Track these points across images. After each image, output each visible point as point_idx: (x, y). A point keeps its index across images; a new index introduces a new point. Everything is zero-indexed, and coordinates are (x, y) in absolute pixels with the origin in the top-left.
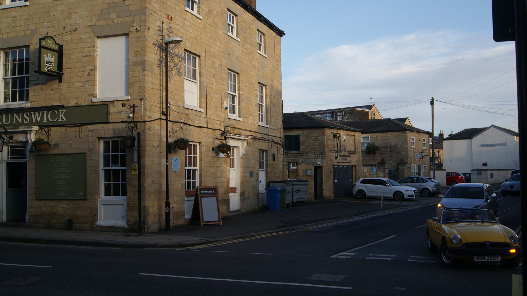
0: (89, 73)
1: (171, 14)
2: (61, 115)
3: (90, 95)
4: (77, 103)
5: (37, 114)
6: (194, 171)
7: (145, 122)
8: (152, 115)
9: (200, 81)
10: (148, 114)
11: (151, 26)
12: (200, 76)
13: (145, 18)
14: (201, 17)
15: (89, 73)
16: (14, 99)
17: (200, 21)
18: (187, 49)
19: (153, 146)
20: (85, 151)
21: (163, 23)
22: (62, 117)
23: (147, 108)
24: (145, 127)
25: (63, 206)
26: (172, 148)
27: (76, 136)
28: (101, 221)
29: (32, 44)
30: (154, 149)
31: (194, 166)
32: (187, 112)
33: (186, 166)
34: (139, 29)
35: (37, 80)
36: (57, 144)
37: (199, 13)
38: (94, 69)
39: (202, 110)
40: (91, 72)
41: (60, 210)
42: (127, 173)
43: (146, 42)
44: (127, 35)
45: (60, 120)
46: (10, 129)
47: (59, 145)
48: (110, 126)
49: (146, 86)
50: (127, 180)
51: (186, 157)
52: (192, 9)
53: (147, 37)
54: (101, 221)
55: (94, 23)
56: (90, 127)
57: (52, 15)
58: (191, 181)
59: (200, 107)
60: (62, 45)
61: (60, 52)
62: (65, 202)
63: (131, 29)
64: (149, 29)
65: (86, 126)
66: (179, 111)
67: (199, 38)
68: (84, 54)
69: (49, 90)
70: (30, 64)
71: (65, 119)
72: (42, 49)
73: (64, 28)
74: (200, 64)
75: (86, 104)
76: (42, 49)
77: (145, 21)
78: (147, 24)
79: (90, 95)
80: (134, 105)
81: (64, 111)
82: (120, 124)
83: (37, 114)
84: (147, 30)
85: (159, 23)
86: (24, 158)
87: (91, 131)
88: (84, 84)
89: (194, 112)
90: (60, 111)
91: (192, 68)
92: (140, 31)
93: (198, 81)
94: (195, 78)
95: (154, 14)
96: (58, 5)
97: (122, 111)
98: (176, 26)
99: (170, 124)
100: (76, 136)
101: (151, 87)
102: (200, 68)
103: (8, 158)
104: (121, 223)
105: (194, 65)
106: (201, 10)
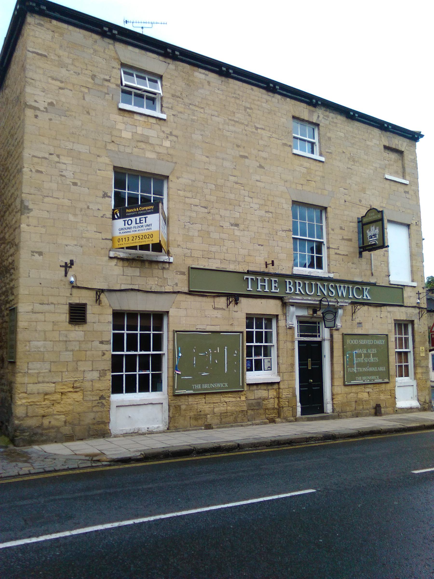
0: (384, 253)
2: (365, 293)
5: (342, 288)
15: (384, 253)
16: (311, 266)
22: (367, 295)
25: (368, 390)
27: (377, 316)
28: (401, 404)
31: (406, 348)
35: (338, 249)
36: (360, 323)
40: (386, 252)
41: (364, 396)
44: (408, 226)
47: (363, 324)
48: (403, 309)
54: (401, 404)
65: (385, 307)
69: (350, 263)
71: (369, 298)
73: (360, 201)
75: (383, 285)
82: (411, 308)
83: (342, 288)
86: (316, 336)
87: (389, 312)
88: (381, 264)
96: (352, 174)
97: (411, 297)
100: (377, 316)
104: (415, 404)
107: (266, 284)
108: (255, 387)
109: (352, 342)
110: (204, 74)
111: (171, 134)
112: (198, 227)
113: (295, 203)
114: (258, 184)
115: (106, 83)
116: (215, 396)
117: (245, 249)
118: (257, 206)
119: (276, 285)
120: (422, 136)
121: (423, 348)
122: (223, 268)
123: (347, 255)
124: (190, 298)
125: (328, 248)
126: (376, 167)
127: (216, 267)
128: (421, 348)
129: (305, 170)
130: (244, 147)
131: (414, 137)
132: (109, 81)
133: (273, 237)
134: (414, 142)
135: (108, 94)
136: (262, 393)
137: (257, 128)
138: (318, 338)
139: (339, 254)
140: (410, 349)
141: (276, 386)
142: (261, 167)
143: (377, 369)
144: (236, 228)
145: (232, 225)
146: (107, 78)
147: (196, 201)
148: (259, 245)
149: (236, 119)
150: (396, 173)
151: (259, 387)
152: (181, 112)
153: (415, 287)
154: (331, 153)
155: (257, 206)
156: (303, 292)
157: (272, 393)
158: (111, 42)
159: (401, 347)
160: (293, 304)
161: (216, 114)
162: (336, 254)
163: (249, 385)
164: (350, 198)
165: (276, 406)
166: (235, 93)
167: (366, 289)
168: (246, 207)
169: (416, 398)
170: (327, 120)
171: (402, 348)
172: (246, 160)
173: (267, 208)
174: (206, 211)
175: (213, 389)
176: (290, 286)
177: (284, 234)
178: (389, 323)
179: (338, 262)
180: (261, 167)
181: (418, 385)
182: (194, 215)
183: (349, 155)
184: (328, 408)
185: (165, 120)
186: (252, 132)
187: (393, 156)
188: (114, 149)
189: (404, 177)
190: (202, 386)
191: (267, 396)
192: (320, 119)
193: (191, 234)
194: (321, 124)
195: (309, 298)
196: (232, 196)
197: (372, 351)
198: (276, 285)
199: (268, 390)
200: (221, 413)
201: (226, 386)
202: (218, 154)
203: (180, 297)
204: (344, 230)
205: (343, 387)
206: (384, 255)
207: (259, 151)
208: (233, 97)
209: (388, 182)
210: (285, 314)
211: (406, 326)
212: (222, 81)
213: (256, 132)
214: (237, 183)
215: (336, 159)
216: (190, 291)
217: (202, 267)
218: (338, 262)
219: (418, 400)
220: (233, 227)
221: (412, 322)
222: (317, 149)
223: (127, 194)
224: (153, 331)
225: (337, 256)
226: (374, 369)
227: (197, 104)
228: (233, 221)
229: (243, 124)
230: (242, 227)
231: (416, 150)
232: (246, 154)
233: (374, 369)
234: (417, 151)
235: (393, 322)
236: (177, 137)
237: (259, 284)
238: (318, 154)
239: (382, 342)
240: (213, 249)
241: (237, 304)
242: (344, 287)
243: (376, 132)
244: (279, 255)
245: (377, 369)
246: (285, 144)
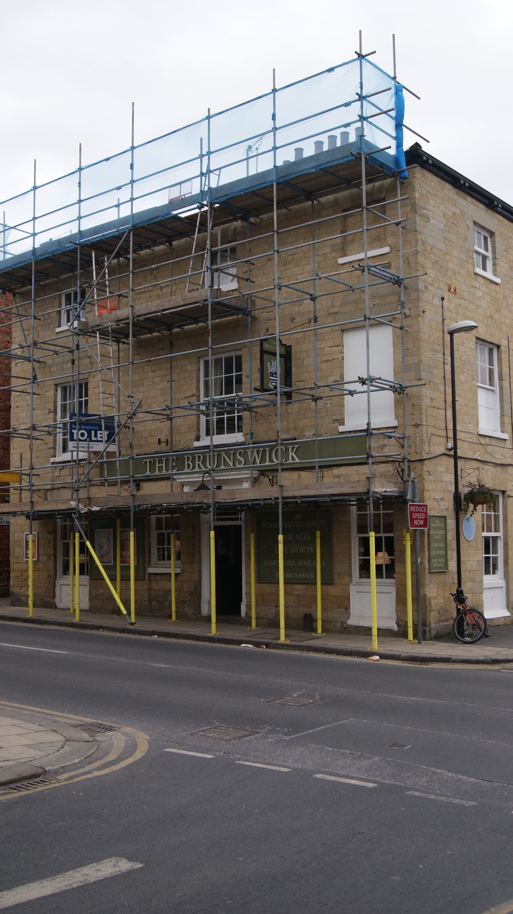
1: (455, 284)
3: (335, 421)
5: (255, 454)
6: (495, 539)
7: (422, 460)
8: (432, 449)
9: (501, 388)
10: (426, 447)
11: (427, 308)
12: (501, 379)
13: (418, 295)
14: (498, 280)
16: (220, 431)
17: (497, 288)
18: (481, 337)
19: (434, 499)
21: (443, 299)
23: (425, 438)
24: (422, 470)
26: (462, 502)
30: (436, 504)
32: (483, 441)
33: (483, 531)
37: (495, 275)
39: (506, 436)
42: (395, 543)
43: (421, 334)
45: (290, 461)
46: (219, 476)
49: (423, 404)
50: (396, 553)
51: (483, 515)
52: (484, 268)
53: (421, 326)
55: (337, 309)
56: (336, 471)
58: (491, 555)
59: (503, 432)
60: (290, 346)
61: (287, 356)
64: (424, 312)
66: (471, 440)
67: (497, 316)
68: (324, 359)
70: (244, 377)
71: (297, 460)
72: (265, 355)
73: (292, 319)
74: (500, 360)
76: (265, 356)
77: (418, 300)
78: (421, 304)
79: (335, 421)
81: (296, 446)
84: (422, 313)
85: (437, 301)
89: (493, 442)
90: (290, 447)
91: (487, 366)
92: (409, 316)
93: (497, 388)
94: (491, 383)
95: (430, 287)
97: (385, 445)
98: (462, 301)
99: (460, 463)
101: (429, 404)
102: (500, 366)
105: (491, 363)
106: (498, 269)
107: (164, 465)
108: (159, 576)
118: (160, 378)
119: (174, 464)
151: (164, 576)
155: (160, 378)
159: (489, 530)
163: (150, 574)
167: (293, 448)
176: (189, 462)
195: (196, 475)
197: (303, 537)
237: (157, 465)
242: (258, 452)
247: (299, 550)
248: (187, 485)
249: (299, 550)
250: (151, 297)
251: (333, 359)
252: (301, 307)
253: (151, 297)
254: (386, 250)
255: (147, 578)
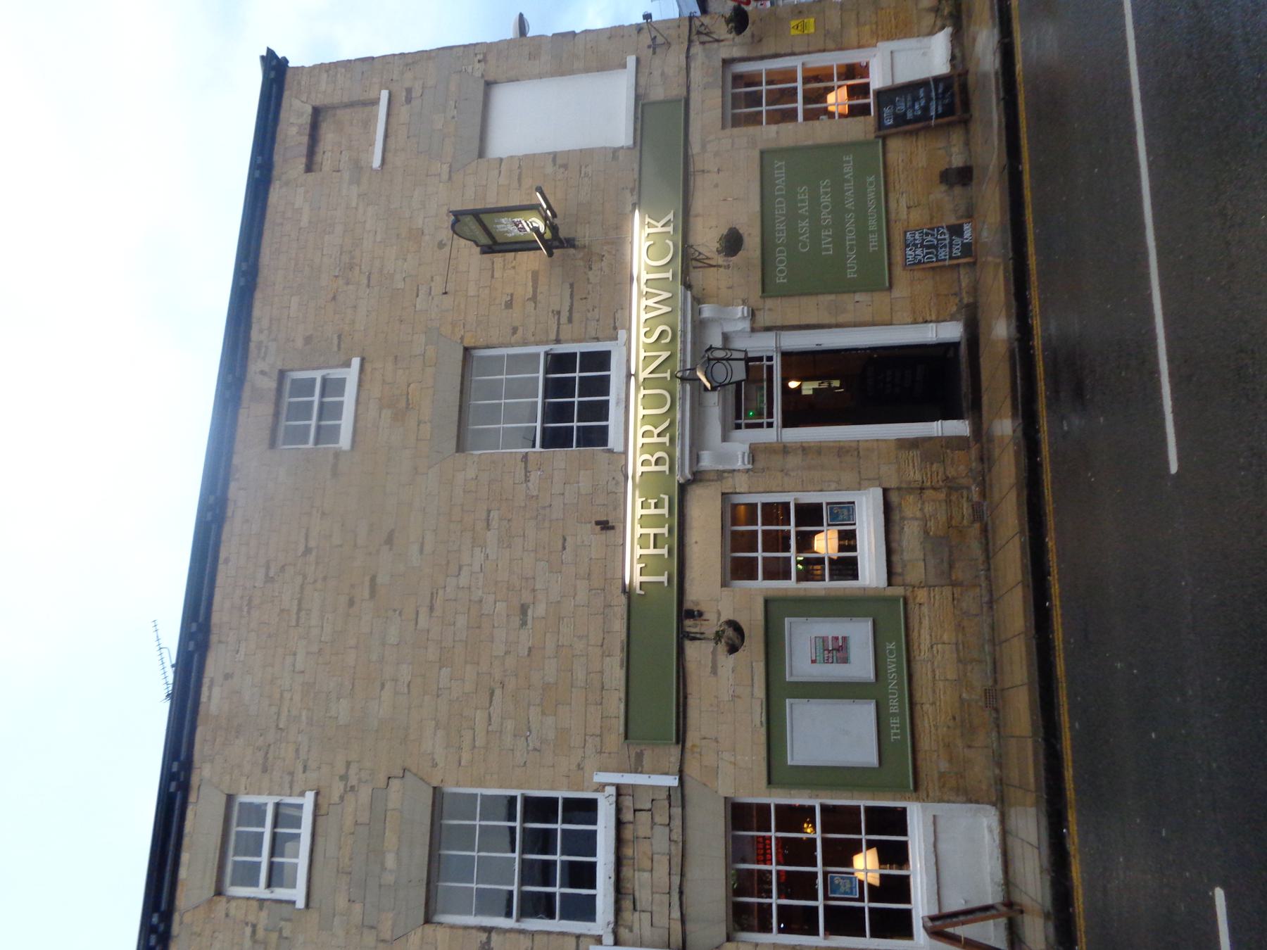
0: (561, 166)
4: (632, 190)
15: (561, 166)
20: (757, 154)
27: (716, 186)
29: (462, 338)
34: (480, 57)
35: (559, 313)
38: (555, 156)
40: (559, 162)
44: (489, 85)
48: (695, 97)
55: (446, 168)
56: (695, 148)
57: (400, 285)
62: (893, 205)
63: (478, 74)
71: (671, 216)
75: (636, 166)
80: (649, 47)
86: (770, 368)
87: (704, 146)
88: (586, 175)
97: (663, 74)
100: (716, 186)
103: (770, 425)
108: (895, 558)
109: (781, 267)
110: (210, 688)
111: (344, 778)
112: (534, 713)
113: (460, 447)
114: (428, 548)
115: (261, 933)
116: (916, 677)
117: (575, 587)
118: (477, 550)
120: (270, 52)
121: (793, 23)
122: (622, 650)
123: (572, 286)
124: (692, 737)
125: (558, 341)
126: (359, 196)
127: (621, 666)
128: (793, 32)
129: (387, 413)
130: (352, 586)
131: (276, 70)
132: (254, 926)
133: (544, 508)
134: (289, 75)
135: (281, 930)
136: (910, 536)
137: (307, 551)
138: (774, 362)
139: (571, 311)
140: (796, 63)
141: (894, 498)
142: (389, 541)
143: (848, 181)
144: (530, 612)
145: (524, 623)
146: (248, 930)
147: (480, 716)
148: (564, 548)
149: (295, 608)
150: (368, 124)
151: (894, 545)
152: (297, 751)
153: (638, 61)
154: (339, 337)
155: (477, 550)
156: (666, 424)
157: (910, 508)
158: (176, 917)
160: (695, 458)
161: (289, 660)
162: (570, 320)
164: (438, 278)
165: (942, 496)
166: (241, 609)
168: (480, 584)
169: (926, 40)
170: (267, 347)
171: (795, 110)
172: (379, 580)
173: (480, 525)
174: (498, 692)
175: (900, 683)
176: (653, 460)
177: (535, 476)
178: (733, 144)
179: (589, 315)
180: (389, 541)
181: (890, 37)
182: (509, 725)
183: (341, 282)
184: (951, 331)
185: (317, 794)
186: (317, 563)
187: (328, 137)
188: (390, 923)
189: (376, 102)
190: (894, 715)
191: (916, 523)
192: (266, 369)
193: (551, 735)
194: (279, 365)
196: (461, 621)
197: (802, 201)
198: (652, 502)
199: (903, 518)
200: (959, 661)
201: (891, 646)
202: (374, 657)
203: (692, 769)
204: (512, 295)
205: (896, 293)
206: (565, 166)
207: (355, 545)
208: (249, 612)
209: (389, 155)
210: (720, 475)
211: (739, 79)
212: (220, 642)
213: (314, 553)
214: (432, 608)
215: (353, 322)
216: (677, 742)
217: (622, 706)
218: (589, 315)
219: (932, 33)
220: (530, 622)
221: (726, 63)
222: (335, 373)
223: (482, 854)
224: (770, 830)
225: (576, 316)
226: (849, 187)
227: (274, 709)
228: (516, 621)
229: (302, 587)
230: (526, 597)
231: (307, 65)
232: (367, 579)
233: (849, 187)
234: (308, 62)
235: (728, 131)
236: (348, 764)
238: (347, 370)
239: (779, 168)
240: (580, 675)
241: (700, 614)
243: (276, 195)
244: (583, 492)
245: (848, 181)
246: (335, 473)
247: (826, 207)
248: (698, 459)
249: (826, 207)
250: (315, 581)
251: (520, 167)
252: (426, 231)
253: (315, 581)
254: (384, 95)
255: (898, 591)
